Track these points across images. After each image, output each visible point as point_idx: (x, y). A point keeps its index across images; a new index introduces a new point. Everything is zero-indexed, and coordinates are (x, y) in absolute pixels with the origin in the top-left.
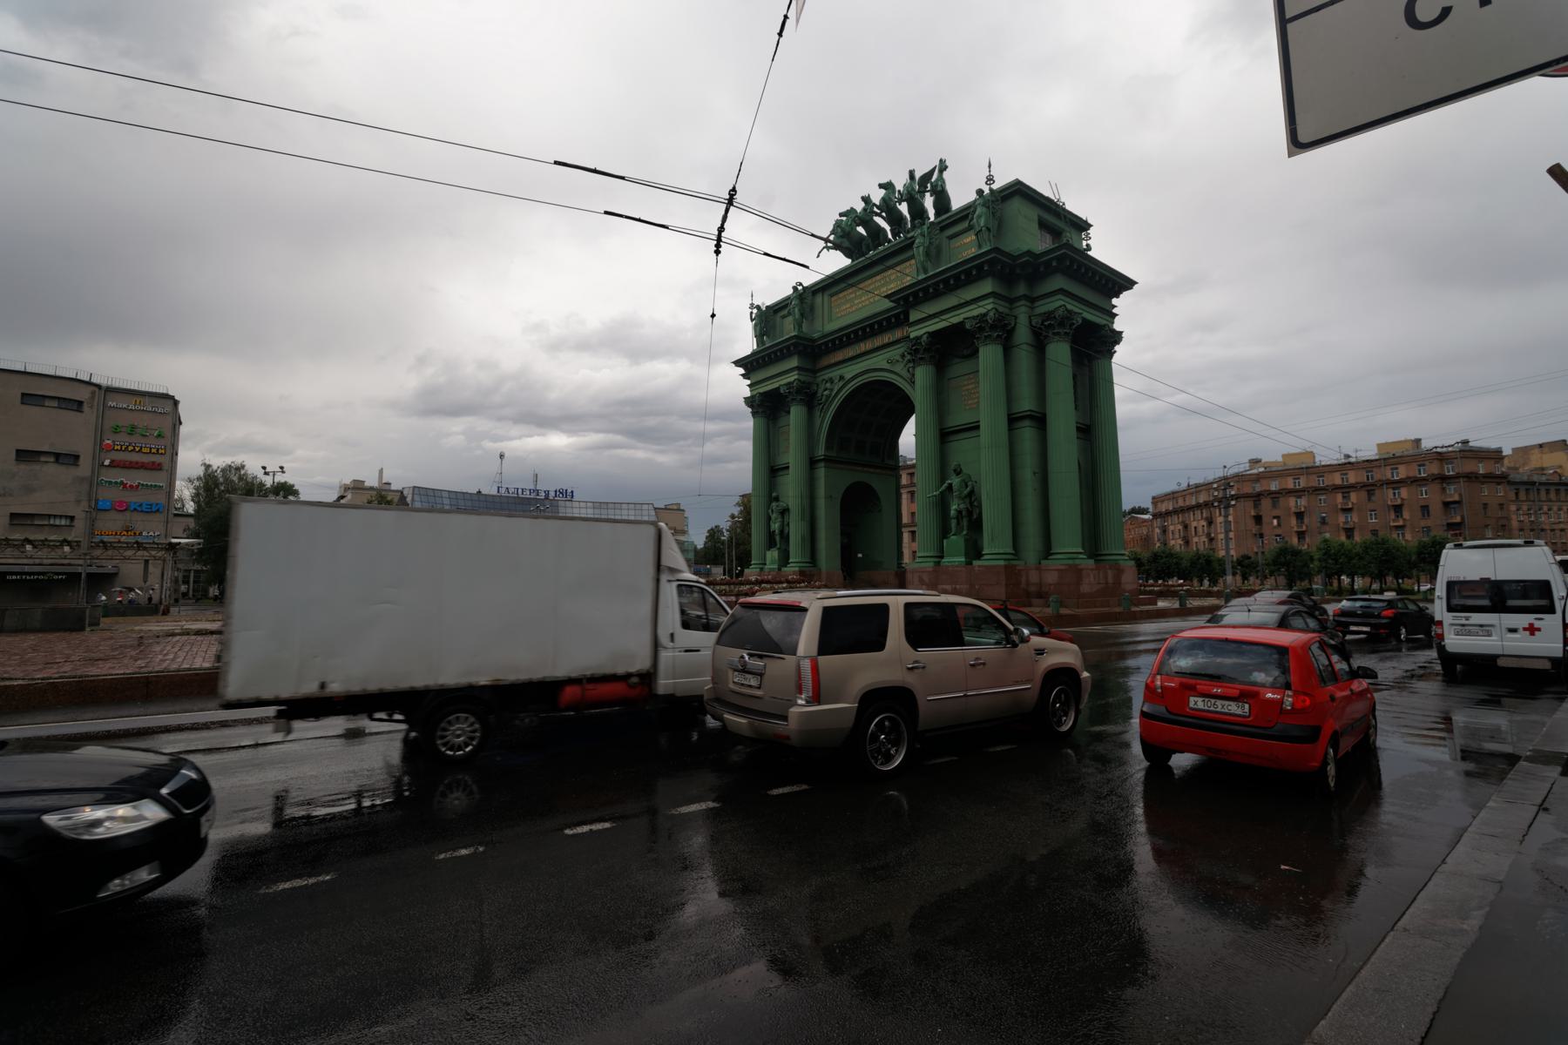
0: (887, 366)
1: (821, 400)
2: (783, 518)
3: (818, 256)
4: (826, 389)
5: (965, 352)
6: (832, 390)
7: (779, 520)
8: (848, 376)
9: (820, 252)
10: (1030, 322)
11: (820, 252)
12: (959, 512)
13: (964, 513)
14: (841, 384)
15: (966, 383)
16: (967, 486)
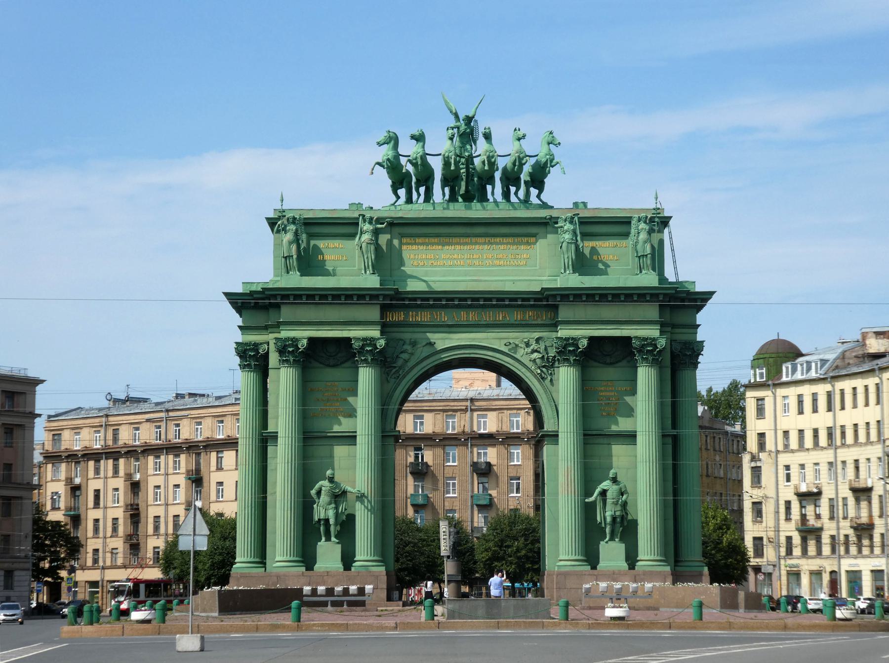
0: (505, 349)
1: (395, 363)
2: (336, 503)
3: (372, 173)
4: (402, 352)
5: (608, 361)
6: (412, 354)
7: (333, 505)
8: (440, 346)
9: (373, 169)
10: (671, 348)
11: (373, 169)
12: (614, 519)
13: (618, 520)
14: (427, 351)
15: (603, 388)
16: (622, 495)
